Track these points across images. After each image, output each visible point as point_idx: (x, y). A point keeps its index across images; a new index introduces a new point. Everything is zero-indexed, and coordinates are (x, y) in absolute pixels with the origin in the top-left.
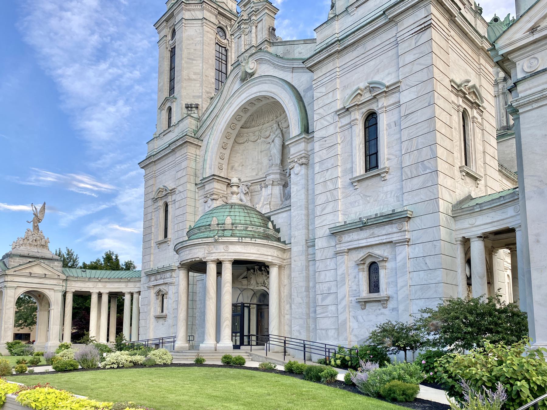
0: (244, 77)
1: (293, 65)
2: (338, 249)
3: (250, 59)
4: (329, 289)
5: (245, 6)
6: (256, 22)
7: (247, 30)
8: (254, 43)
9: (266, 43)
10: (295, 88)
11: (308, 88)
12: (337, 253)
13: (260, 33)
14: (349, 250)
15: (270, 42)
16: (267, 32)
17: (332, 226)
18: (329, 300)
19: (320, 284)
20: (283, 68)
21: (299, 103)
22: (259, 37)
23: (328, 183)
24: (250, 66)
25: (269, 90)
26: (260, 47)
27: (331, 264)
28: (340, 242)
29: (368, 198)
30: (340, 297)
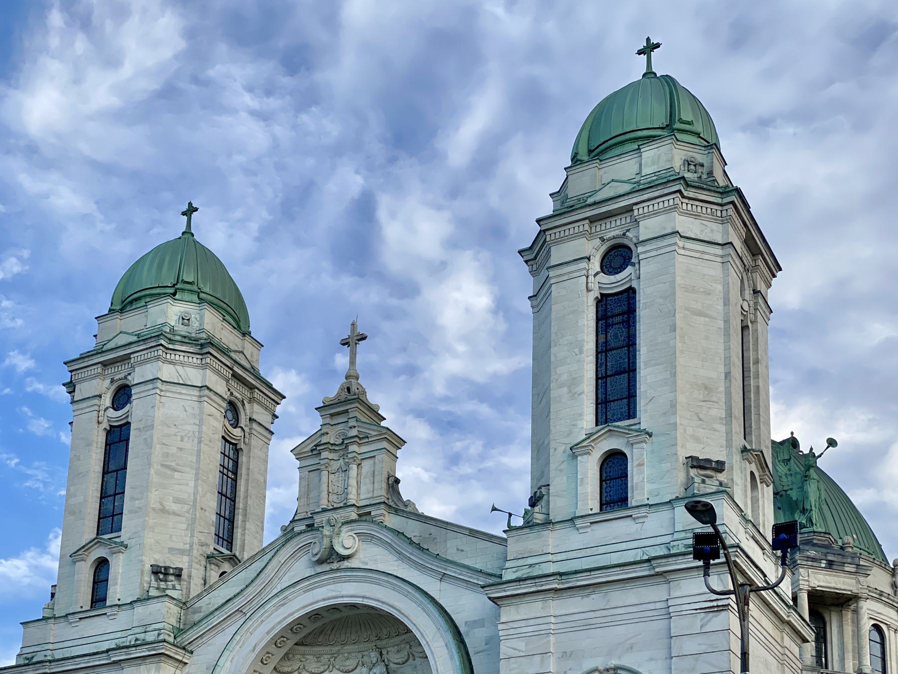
0: (324, 558)
1: (446, 569)
3: (345, 529)
5: (332, 415)
6: (360, 457)
7: (335, 466)
8: (353, 499)
9: (382, 506)
10: (446, 611)
11: (475, 622)
13: (367, 480)
15: (390, 506)
16: (384, 485)
21: (459, 647)
22: (363, 488)
24: (346, 542)
26: (367, 510)
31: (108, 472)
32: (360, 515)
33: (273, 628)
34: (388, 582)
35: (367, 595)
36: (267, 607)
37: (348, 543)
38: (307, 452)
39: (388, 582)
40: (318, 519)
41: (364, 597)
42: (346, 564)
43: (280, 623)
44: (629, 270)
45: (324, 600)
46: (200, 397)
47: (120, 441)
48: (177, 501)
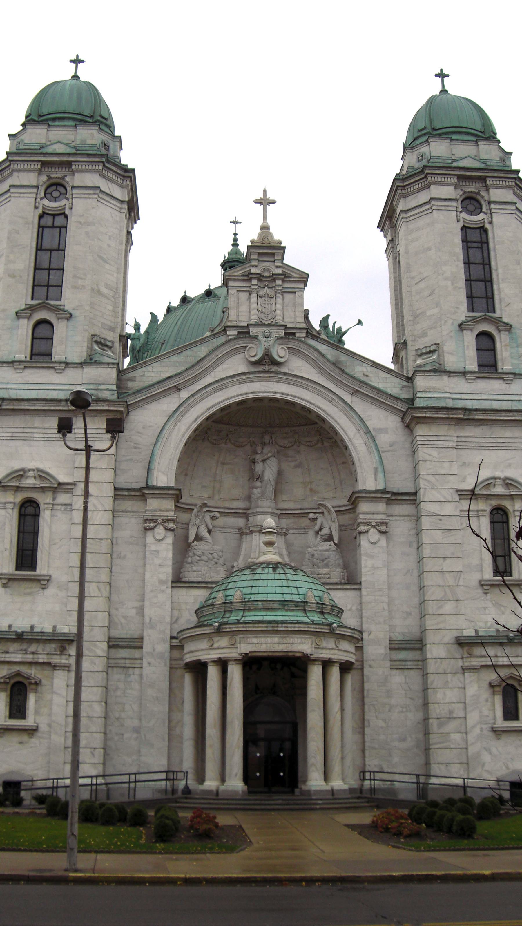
2: (466, 664)
4: (451, 712)
12: (464, 669)
14: (482, 666)
17: (456, 634)
18: (451, 726)
19: (436, 705)
20: (339, 383)
23: (447, 575)
24: (279, 352)
25: (312, 401)
27: (455, 681)
28: (471, 655)
29: (502, 608)
30: (470, 722)
31: (41, 249)
32: (285, 333)
33: (213, 406)
34: (315, 388)
35: (297, 395)
36: (208, 389)
37: (282, 353)
38: (238, 276)
39: (315, 388)
40: (253, 331)
41: (294, 396)
42: (275, 368)
43: (219, 403)
44: (64, 202)
45: (259, 392)
46: (121, 208)
47: (53, 227)
48: (107, 286)
